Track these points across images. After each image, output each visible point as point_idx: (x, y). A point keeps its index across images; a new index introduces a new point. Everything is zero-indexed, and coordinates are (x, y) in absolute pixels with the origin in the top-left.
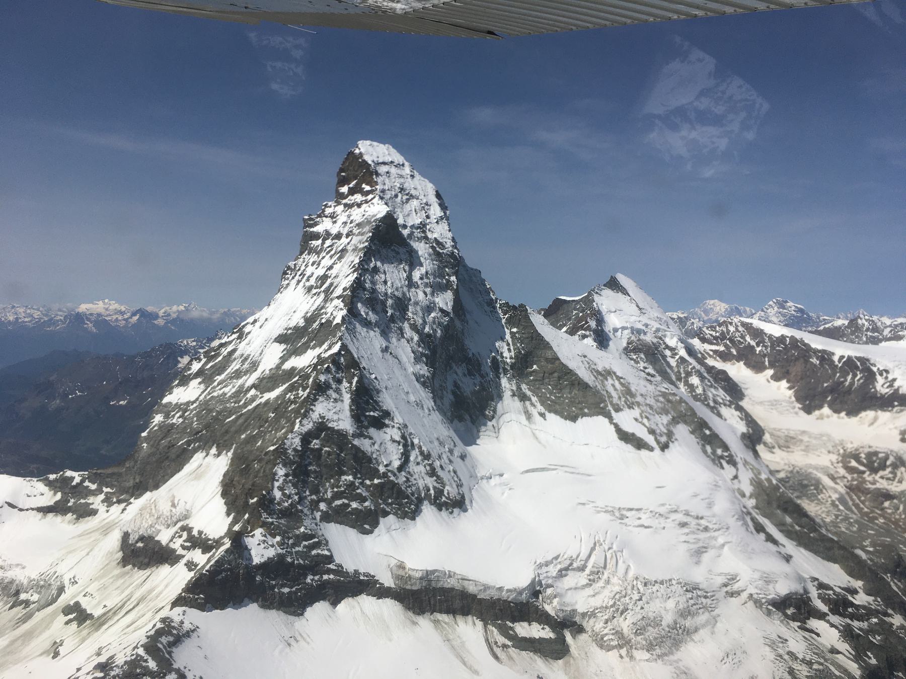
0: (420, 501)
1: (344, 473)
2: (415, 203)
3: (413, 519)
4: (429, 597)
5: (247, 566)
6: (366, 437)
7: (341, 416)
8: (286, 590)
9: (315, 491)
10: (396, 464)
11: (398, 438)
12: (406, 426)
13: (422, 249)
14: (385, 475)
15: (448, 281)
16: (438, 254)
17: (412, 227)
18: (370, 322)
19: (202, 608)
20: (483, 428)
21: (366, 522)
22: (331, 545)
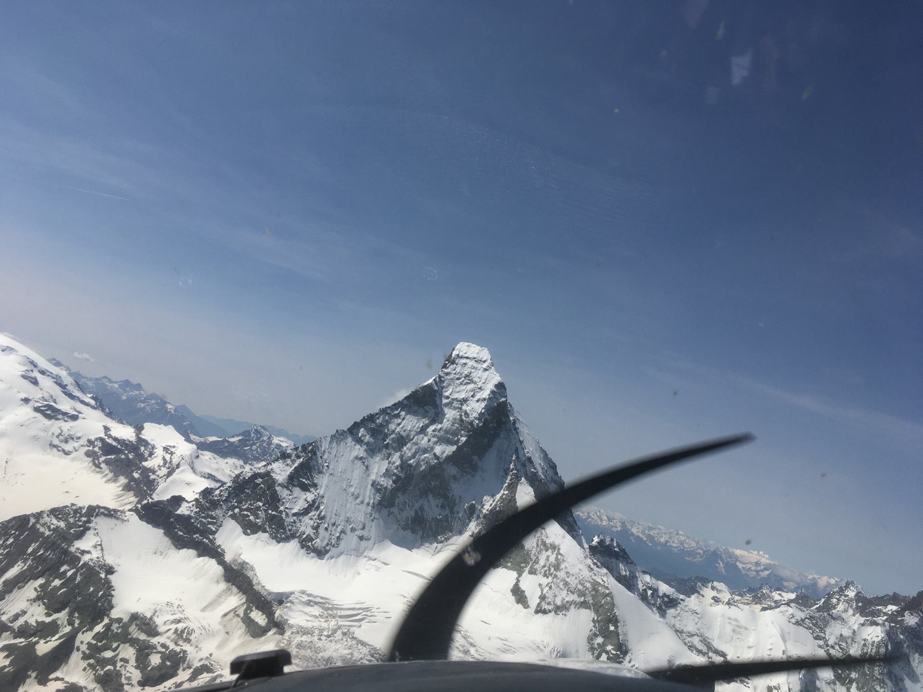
0: (293, 536)
1: (261, 501)
2: (472, 386)
3: (279, 542)
4: (237, 576)
5: (170, 511)
6: (288, 489)
7: (283, 473)
8: (181, 533)
9: (239, 502)
10: (295, 511)
11: (309, 499)
12: (323, 497)
13: (450, 414)
14: (281, 512)
15: (459, 440)
16: (462, 420)
17: (453, 399)
18: (362, 441)
19: (141, 518)
20: (427, 545)
21: (250, 528)
22: (221, 529)
